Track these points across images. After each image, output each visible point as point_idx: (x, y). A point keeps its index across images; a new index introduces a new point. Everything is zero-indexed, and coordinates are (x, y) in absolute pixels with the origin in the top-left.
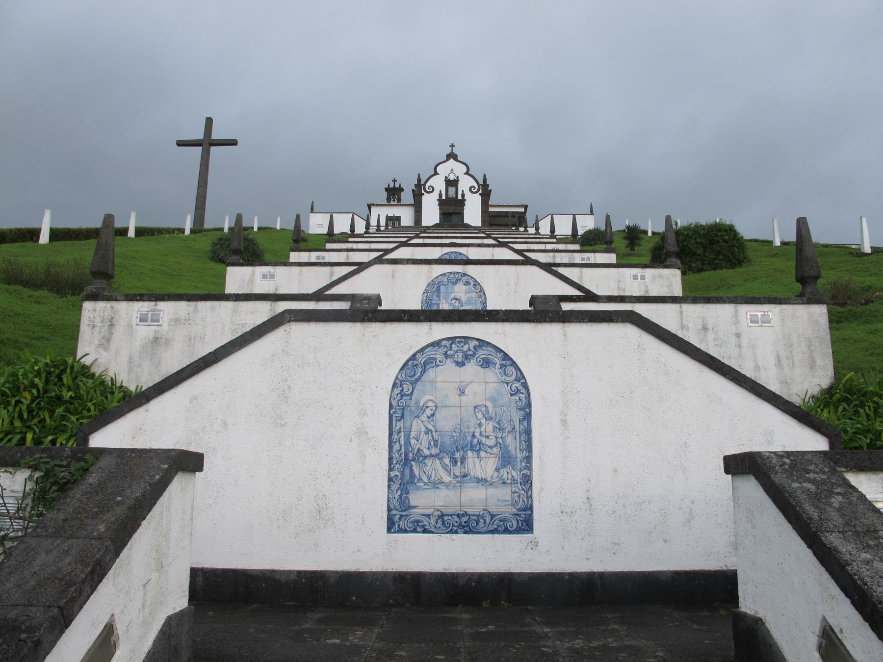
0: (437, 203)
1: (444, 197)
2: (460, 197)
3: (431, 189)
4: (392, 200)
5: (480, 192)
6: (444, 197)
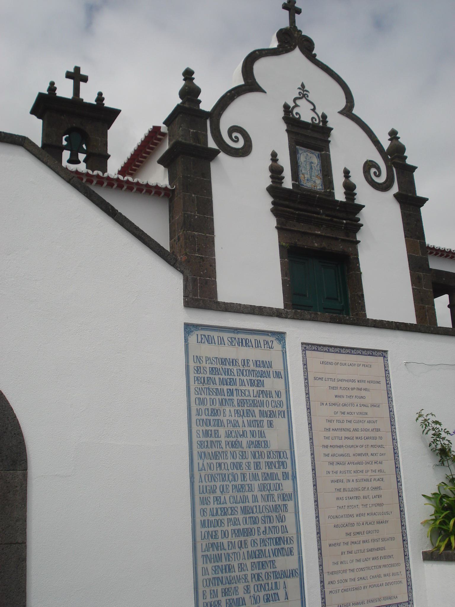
0: (267, 201)
1: (288, 183)
2: (340, 195)
3: (240, 144)
4: (66, 155)
5: (395, 189)
6: (288, 183)
